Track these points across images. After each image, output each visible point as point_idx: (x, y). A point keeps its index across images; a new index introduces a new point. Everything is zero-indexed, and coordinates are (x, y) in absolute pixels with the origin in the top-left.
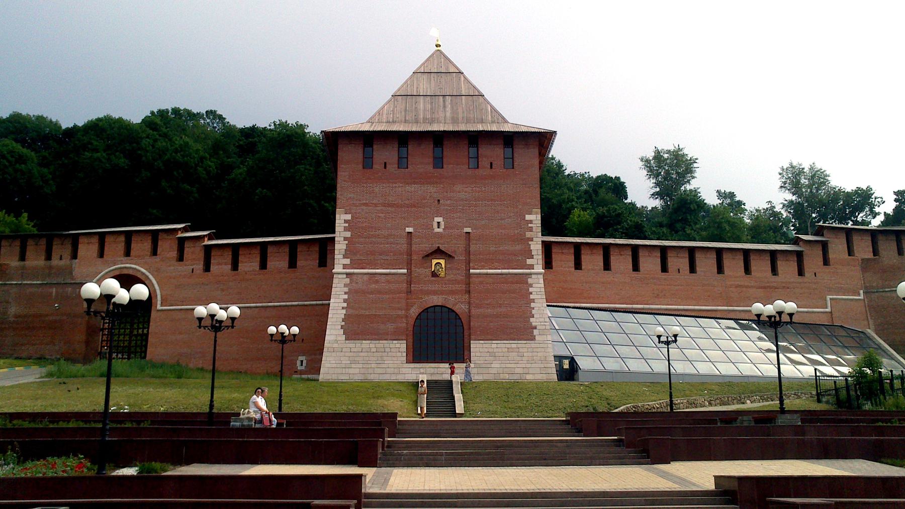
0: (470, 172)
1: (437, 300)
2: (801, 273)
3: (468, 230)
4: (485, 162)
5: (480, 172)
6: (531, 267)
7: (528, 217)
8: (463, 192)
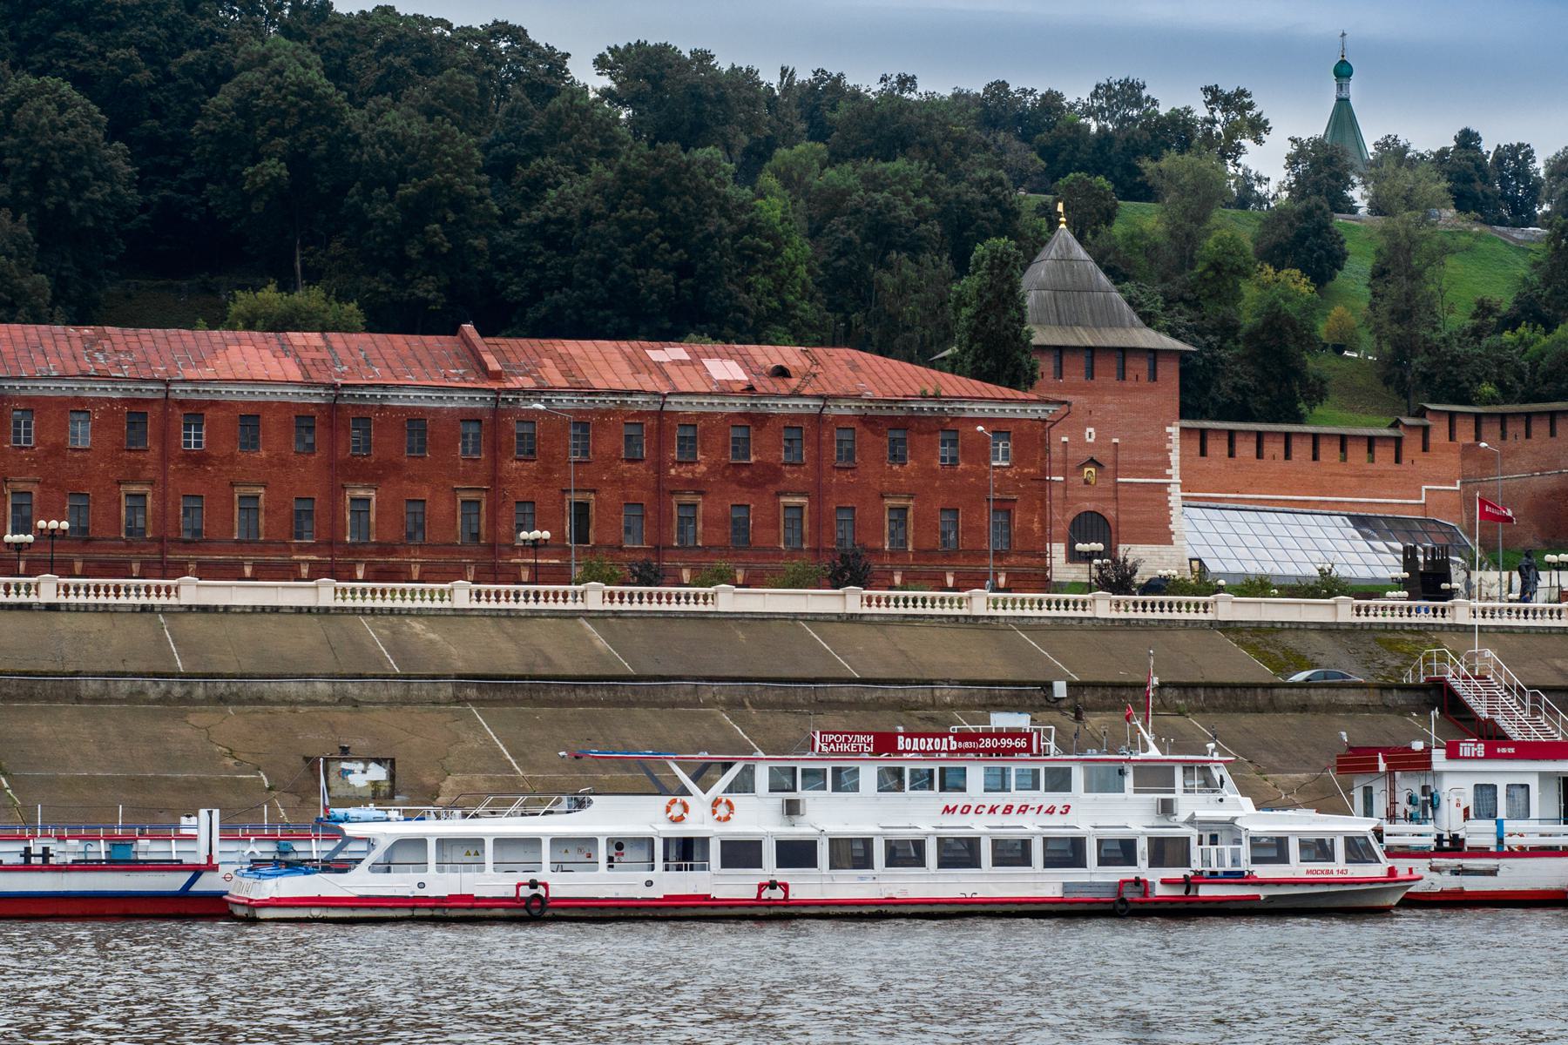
0: (1117, 384)
1: (1089, 506)
2: (1398, 460)
3: (1116, 440)
4: (1130, 374)
5: (1128, 384)
6: (1170, 477)
7: (1169, 429)
8: (1111, 403)
